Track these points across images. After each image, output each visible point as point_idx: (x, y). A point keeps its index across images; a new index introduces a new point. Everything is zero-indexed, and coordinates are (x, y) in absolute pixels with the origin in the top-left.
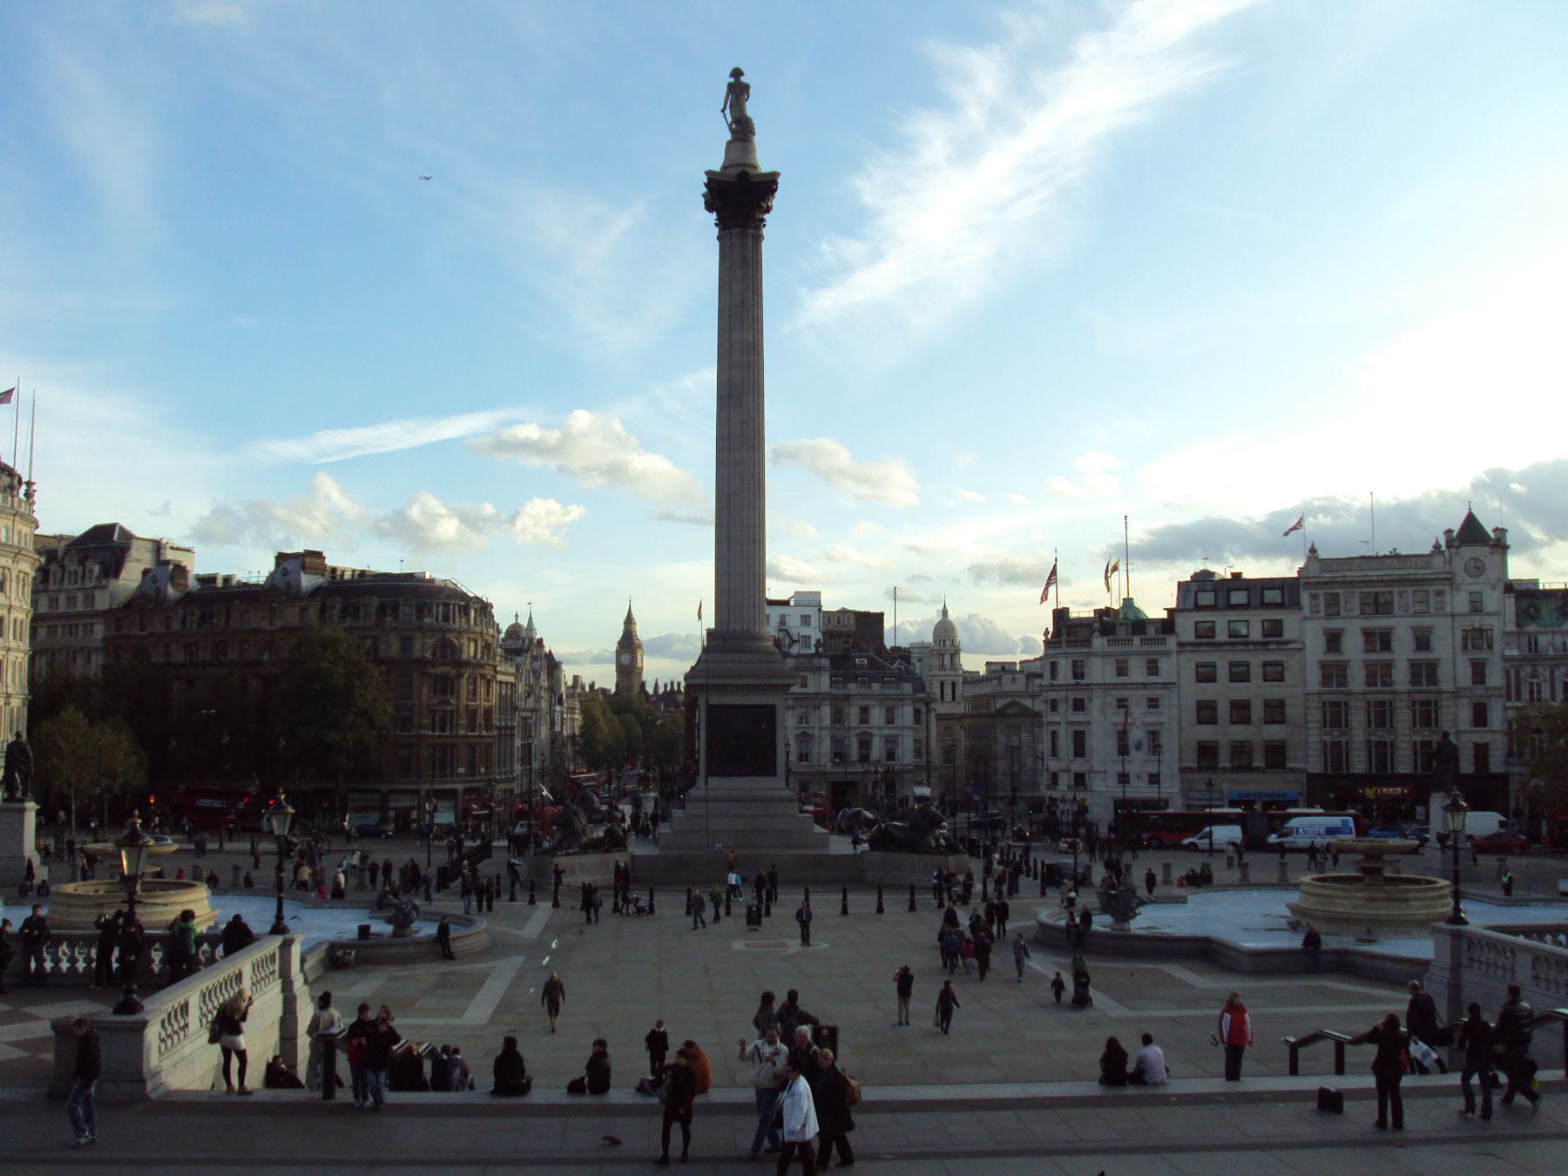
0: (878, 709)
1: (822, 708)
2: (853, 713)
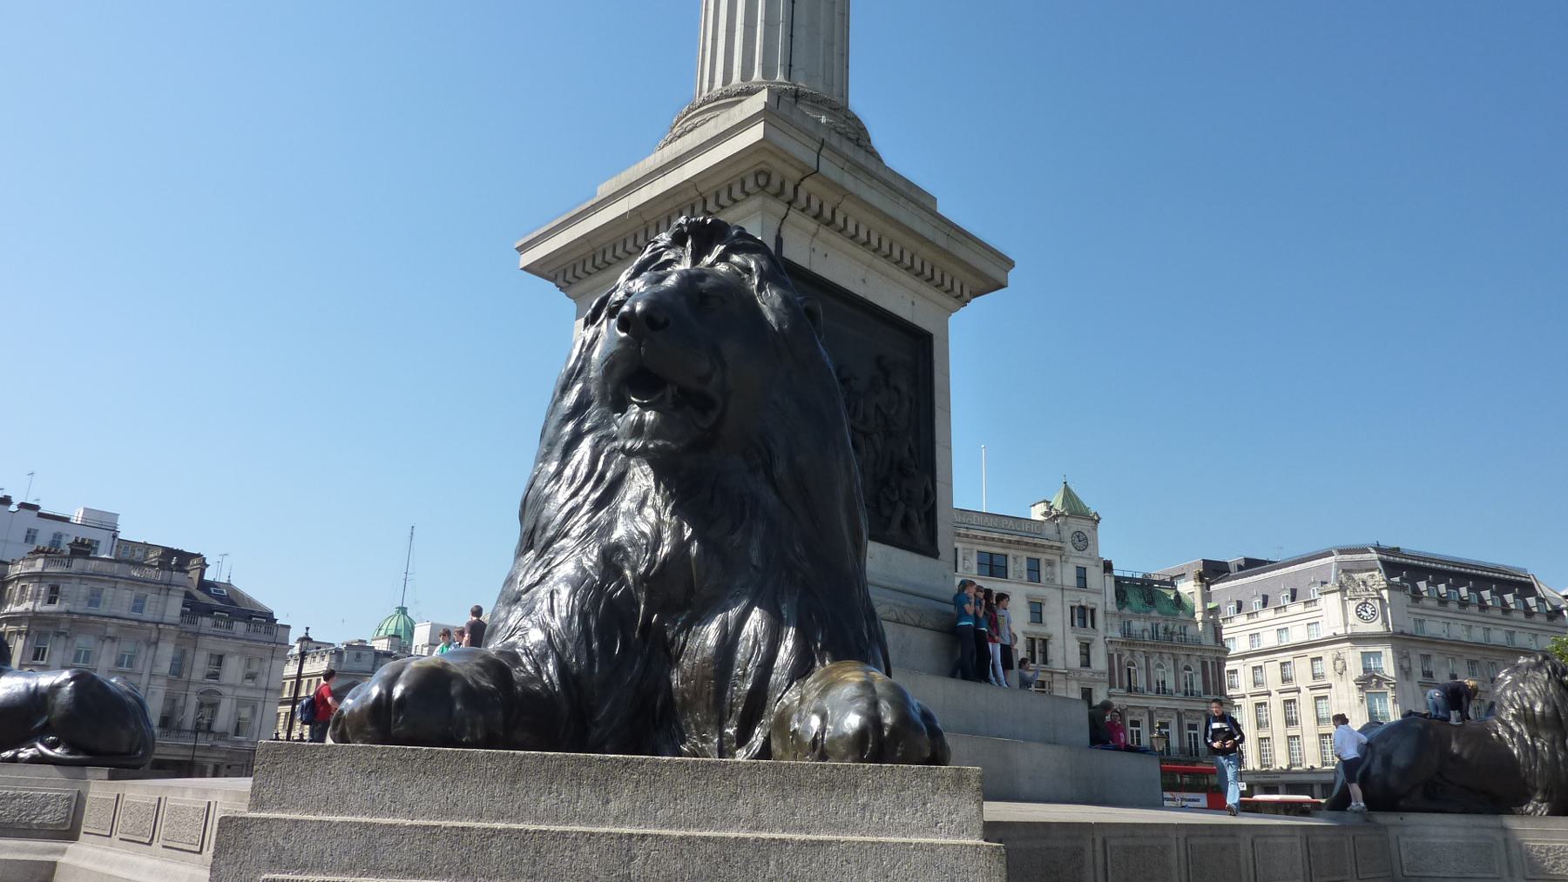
0: (237, 657)
1: (160, 644)
2: (200, 664)
